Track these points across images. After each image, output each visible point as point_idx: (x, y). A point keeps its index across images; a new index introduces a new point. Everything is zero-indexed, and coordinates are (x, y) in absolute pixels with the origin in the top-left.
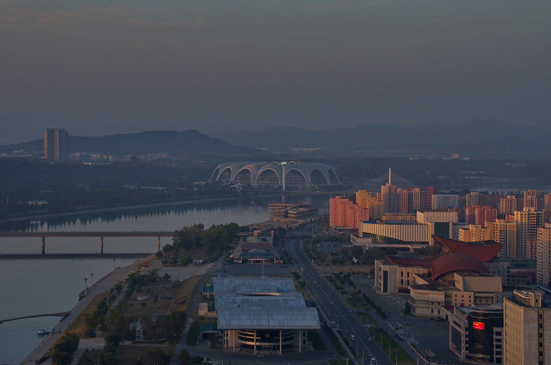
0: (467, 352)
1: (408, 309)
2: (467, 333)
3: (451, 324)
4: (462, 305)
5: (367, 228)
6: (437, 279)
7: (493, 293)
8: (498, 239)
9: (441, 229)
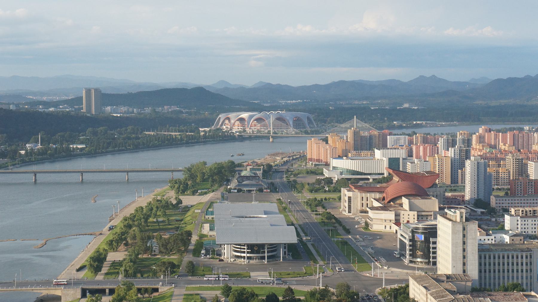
0: (411, 257)
2: (411, 243)
3: (399, 236)
4: (408, 222)
5: (335, 163)
6: (389, 202)
9: (394, 163)
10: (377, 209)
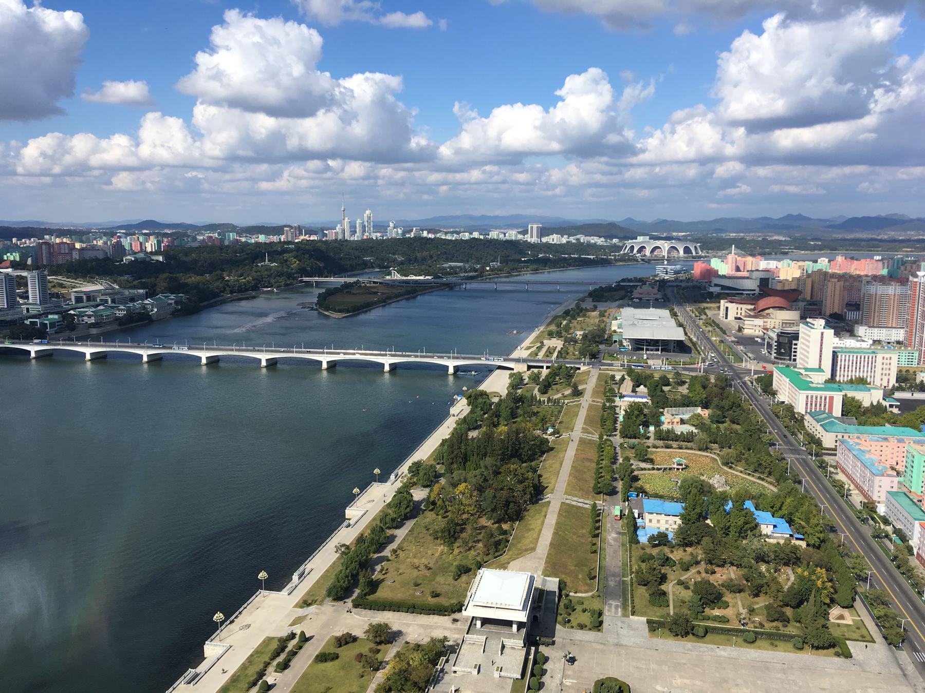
1: (740, 329)
10: (750, 316)
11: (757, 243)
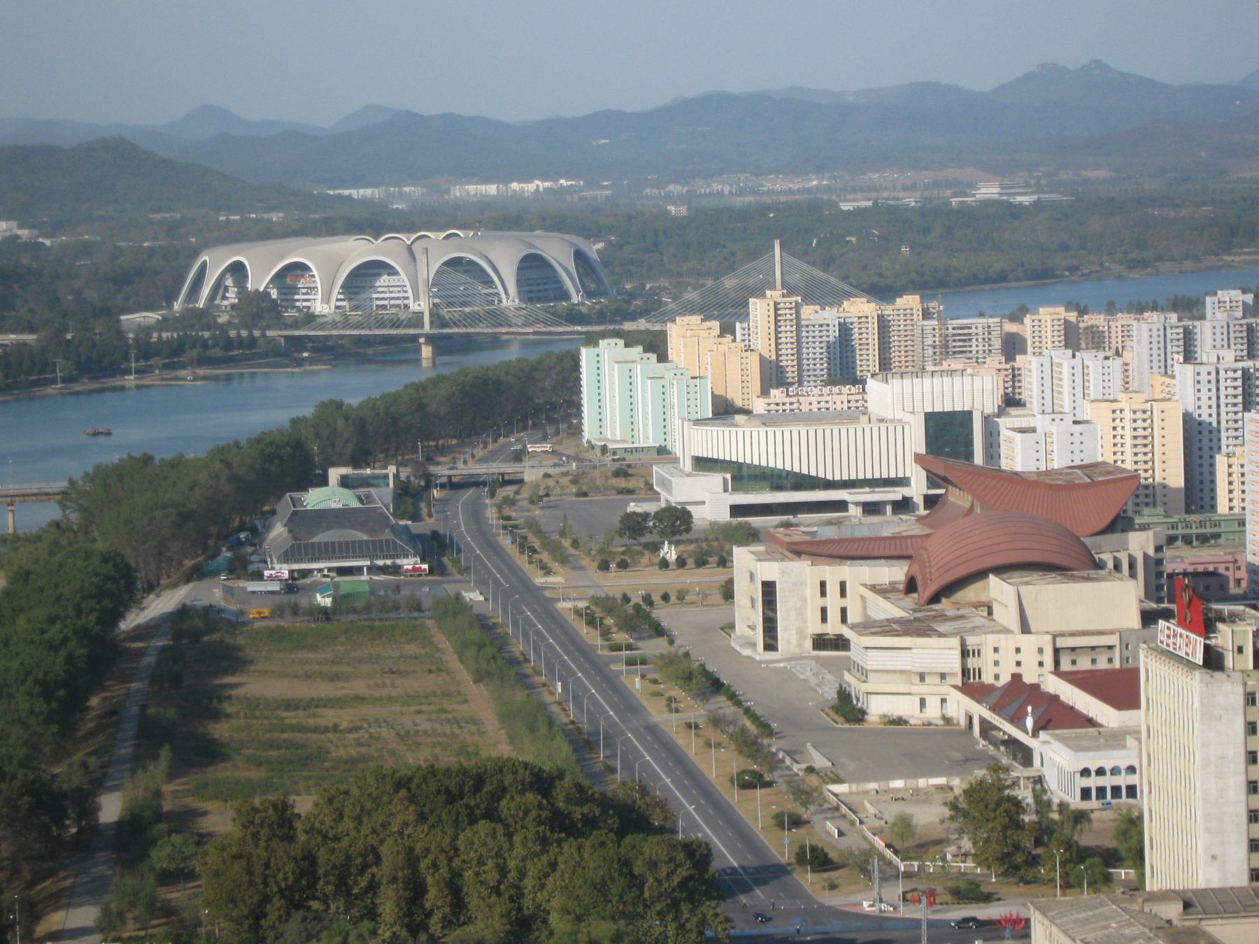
7: (1112, 633)
8: (1128, 457)
9: (947, 433)
11: (892, 221)
